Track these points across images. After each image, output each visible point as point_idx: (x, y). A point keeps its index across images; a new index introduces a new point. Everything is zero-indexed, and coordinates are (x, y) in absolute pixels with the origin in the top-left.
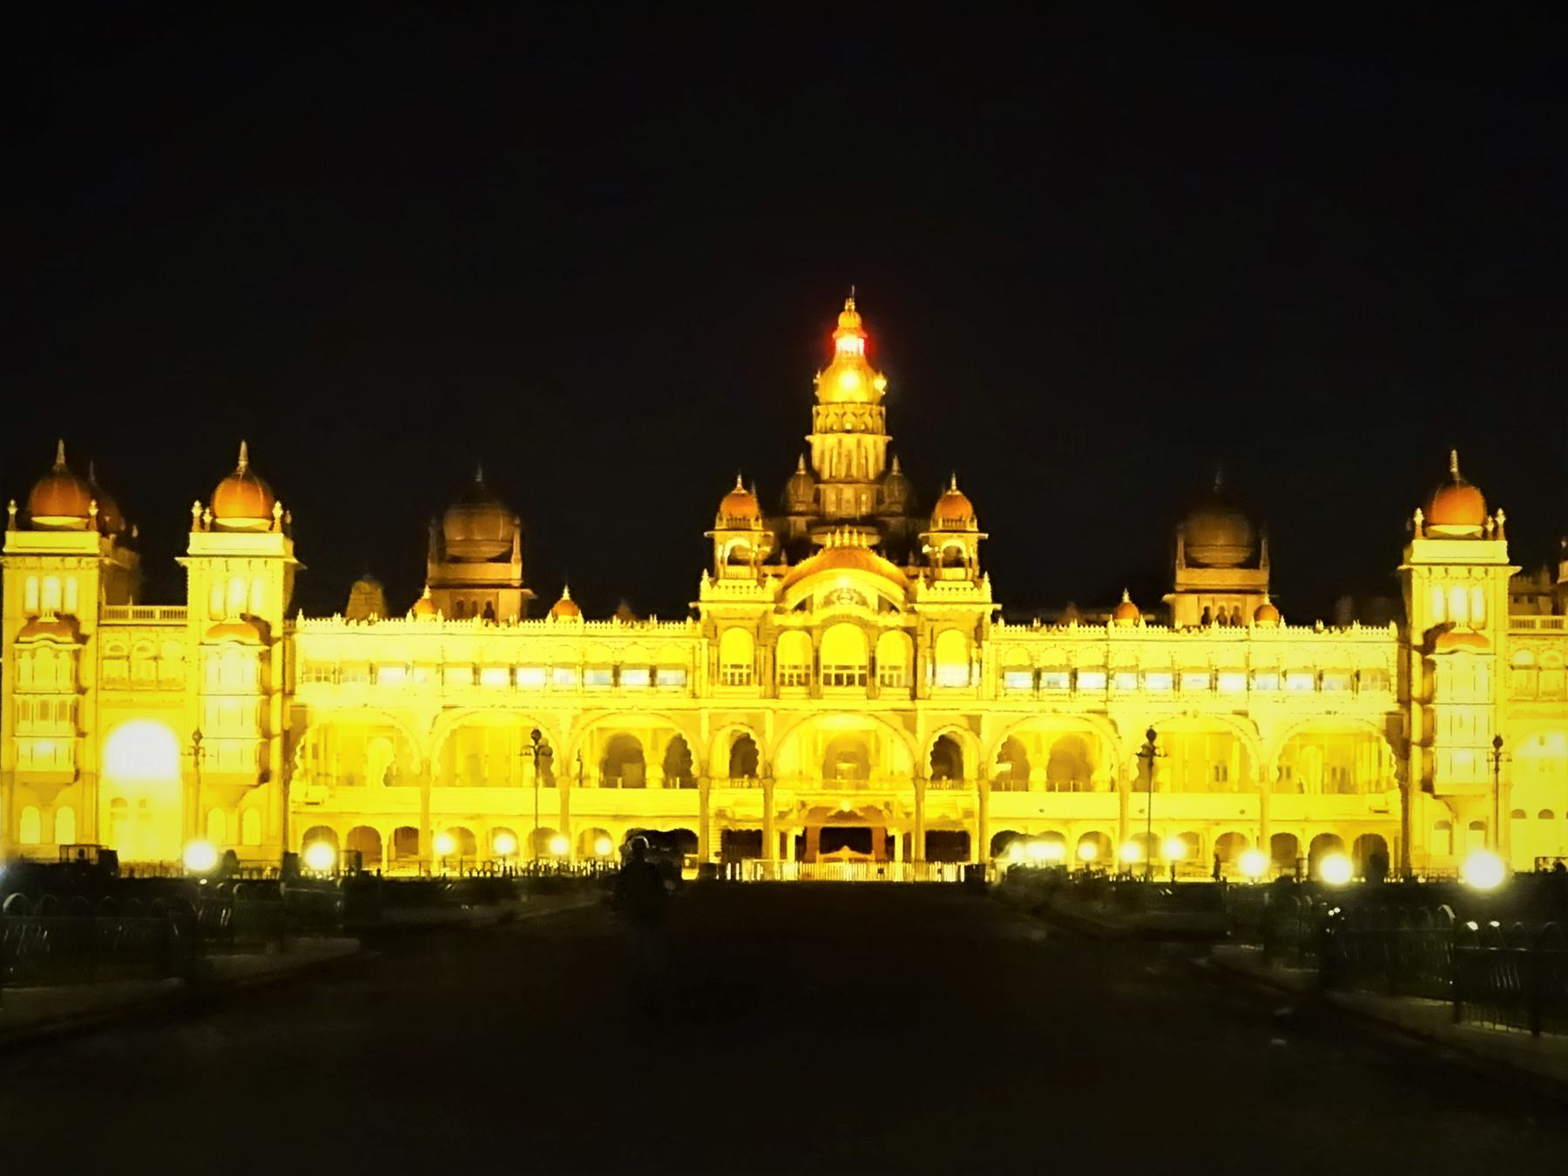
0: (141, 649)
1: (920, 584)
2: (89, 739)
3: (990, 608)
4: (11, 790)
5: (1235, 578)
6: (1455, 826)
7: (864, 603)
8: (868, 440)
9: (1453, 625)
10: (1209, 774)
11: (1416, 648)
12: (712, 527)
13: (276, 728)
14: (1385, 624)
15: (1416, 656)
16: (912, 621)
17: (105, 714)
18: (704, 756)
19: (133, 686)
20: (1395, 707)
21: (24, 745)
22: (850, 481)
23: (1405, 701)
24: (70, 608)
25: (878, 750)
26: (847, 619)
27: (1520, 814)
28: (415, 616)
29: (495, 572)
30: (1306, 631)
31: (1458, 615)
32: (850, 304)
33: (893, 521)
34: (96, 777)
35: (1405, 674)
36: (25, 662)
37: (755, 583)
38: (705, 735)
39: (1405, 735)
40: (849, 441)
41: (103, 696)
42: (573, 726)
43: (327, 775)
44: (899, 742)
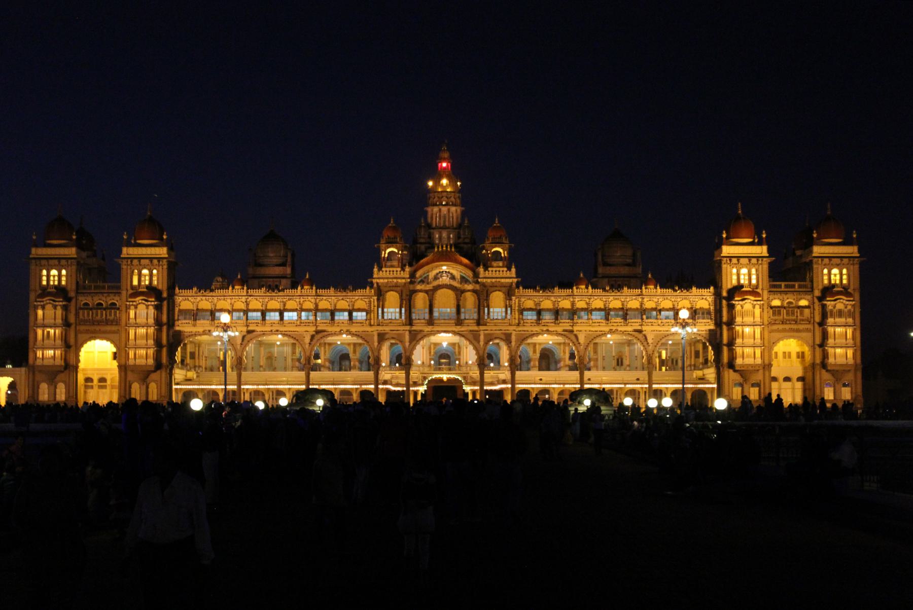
1: (481, 270)
2: (73, 349)
3: (515, 280)
4: (34, 374)
5: (625, 271)
6: (745, 385)
7: (453, 278)
8: (453, 209)
9: (742, 286)
10: (614, 363)
11: (725, 298)
12: (379, 242)
13: (164, 341)
15: (724, 302)
16: (478, 287)
18: (376, 354)
20: (712, 327)
21: (39, 354)
22: (444, 228)
23: (719, 324)
25: (459, 353)
27: (775, 379)
28: (233, 288)
29: (278, 271)
30: (669, 291)
31: (744, 280)
33: (465, 246)
34: (76, 367)
35: (718, 311)
36: (40, 312)
37: (399, 269)
38: (376, 344)
39: (718, 341)
43: (199, 367)
44: (471, 348)
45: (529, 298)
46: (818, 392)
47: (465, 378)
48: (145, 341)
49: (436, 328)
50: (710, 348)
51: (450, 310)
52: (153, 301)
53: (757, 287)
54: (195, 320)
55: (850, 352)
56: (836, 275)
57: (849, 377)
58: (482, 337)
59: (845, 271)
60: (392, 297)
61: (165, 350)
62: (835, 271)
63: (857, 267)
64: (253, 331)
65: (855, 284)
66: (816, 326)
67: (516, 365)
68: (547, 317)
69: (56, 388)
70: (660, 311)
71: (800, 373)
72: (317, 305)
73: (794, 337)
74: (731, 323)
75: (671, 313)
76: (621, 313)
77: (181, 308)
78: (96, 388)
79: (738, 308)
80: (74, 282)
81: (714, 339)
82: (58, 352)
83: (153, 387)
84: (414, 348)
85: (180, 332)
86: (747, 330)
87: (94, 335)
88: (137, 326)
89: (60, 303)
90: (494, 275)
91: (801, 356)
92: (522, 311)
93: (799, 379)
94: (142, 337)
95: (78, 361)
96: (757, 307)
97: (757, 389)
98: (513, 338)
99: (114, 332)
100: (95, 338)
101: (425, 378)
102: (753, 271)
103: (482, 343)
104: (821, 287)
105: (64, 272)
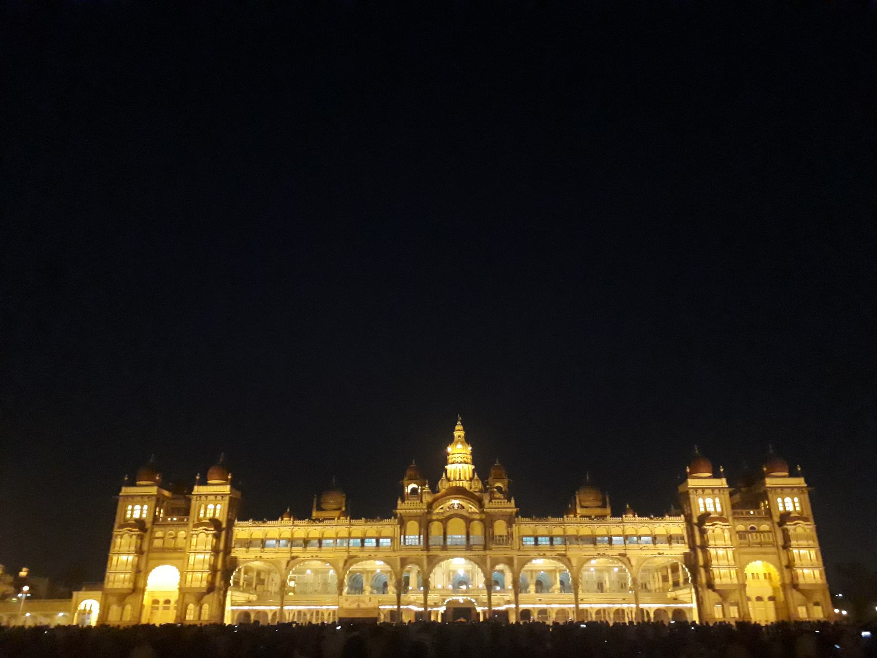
0: (171, 534)
3: (515, 510)
9: (710, 514)
10: (596, 586)
11: (696, 524)
12: (403, 479)
14: (679, 515)
15: (696, 528)
16: (484, 516)
17: (151, 562)
19: (163, 550)
20: (688, 551)
21: (112, 577)
23: (693, 547)
24: (144, 516)
26: (456, 515)
27: (749, 599)
31: (710, 509)
32: (459, 423)
34: (143, 590)
35: (691, 536)
36: (118, 540)
38: (399, 568)
40: (460, 466)
41: (152, 555)
42: (345, 565)
45: (526, 527)
46: (792, 610)
47: (476, 600)
48: (201, 566)
49: (449, 553)
50: (687, 570)
51: (460, 537)
52: (212, 531)
53: (722, 514)
54: (248, 548)
55: (817, 573)
56: (789, 504)
57: (818, 597)
58: (488, 561)
59: (796, 499)
60: (413, 526)
61: (219, 575)
62: (788, 500)
63: (806, 496)
64: (297, 557)
65: (808, 512)
66: (781, 548)
67: (518, 587)
68: (544, 542)
69: (123, 609)
70: (639, 537)
71: (770, 594)
72: (350, 534)
73: (763, 560)
74: (704, 547)
75: (650, 538)
76: (606, 539)
77: (239, 537)
78: (161, 609)
79: (710, 532)
80: (152, 515)
81: (690, 561)
82: (128, 576)
83: (206, 607)
84: (431, 571)
85: (236, 558)
86: (721, 552)
87: (162, 561)
88: (196, 552)
89: (136, 531)
90: (497, 506)
91: (768, 576)
92: (521, 538)
93: (771, 599)
94: (199, 562)
95: (145, 585)
96: (726, 531)
97: (735, 608)
98: (515, 562)
99: (179, 559)
100: (163, 564)
101: (444, 600)
102: (717, 500)
103: (489, 566)
104: (778, 514)
105: (146, 507)
